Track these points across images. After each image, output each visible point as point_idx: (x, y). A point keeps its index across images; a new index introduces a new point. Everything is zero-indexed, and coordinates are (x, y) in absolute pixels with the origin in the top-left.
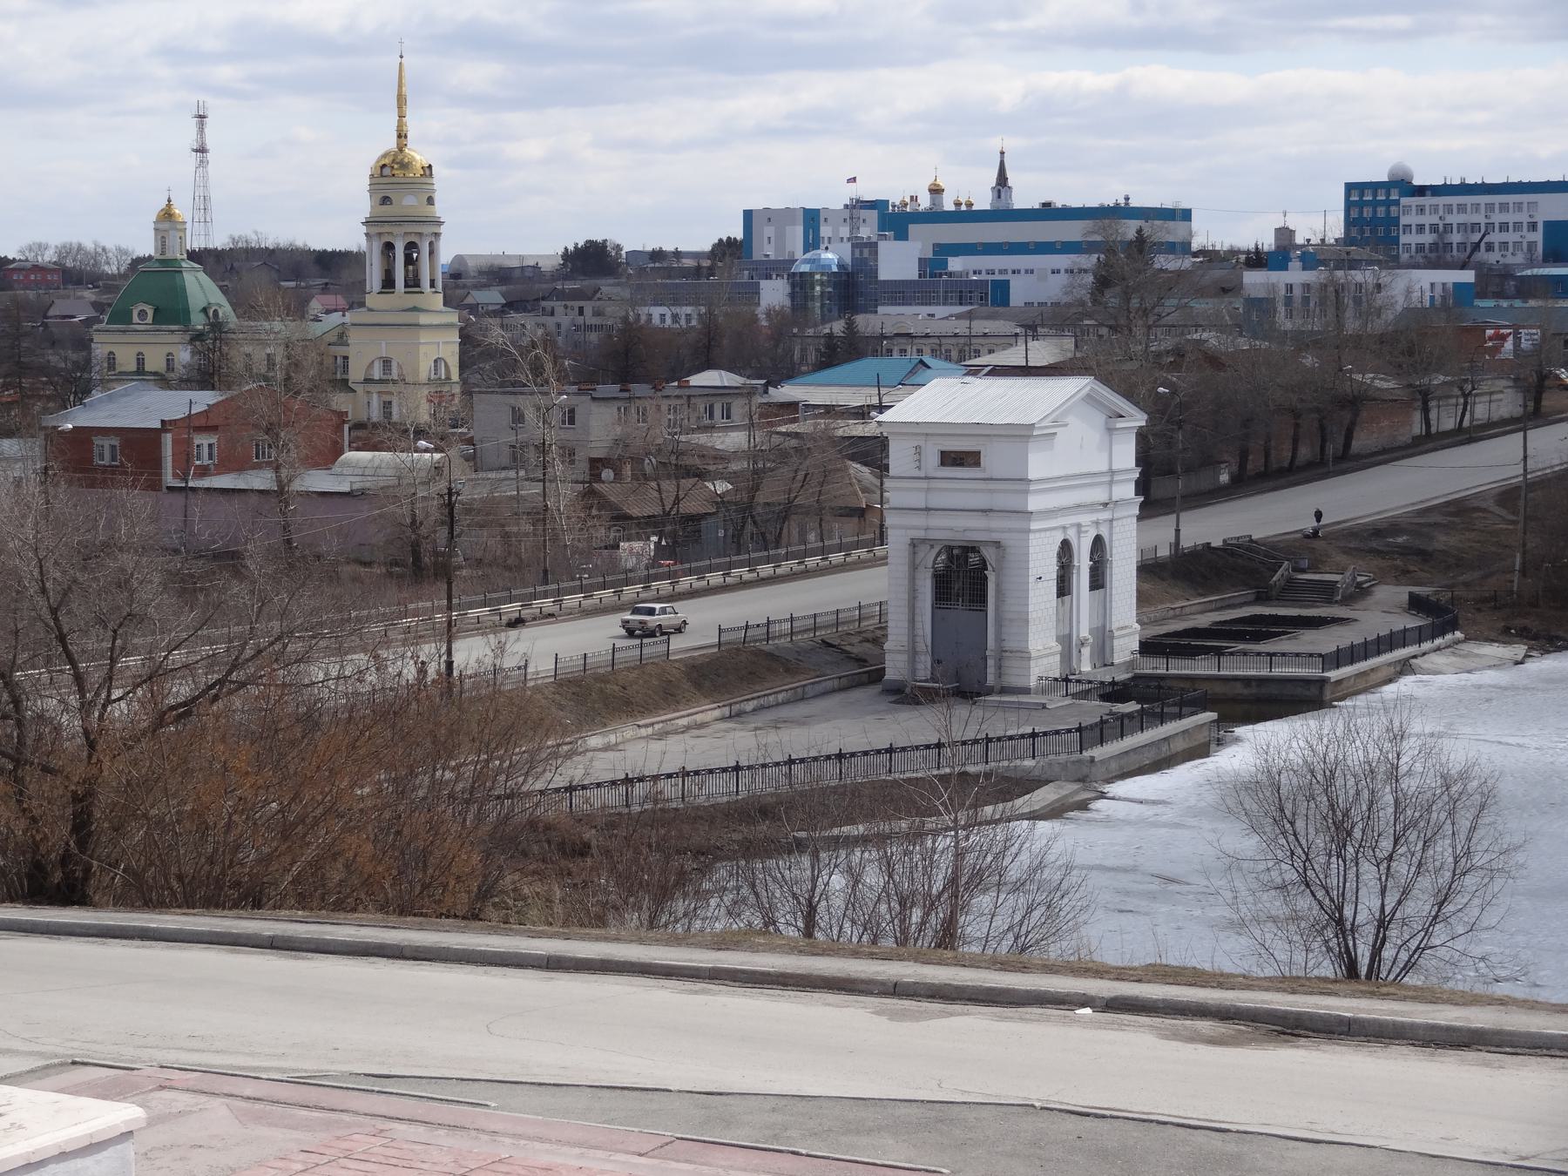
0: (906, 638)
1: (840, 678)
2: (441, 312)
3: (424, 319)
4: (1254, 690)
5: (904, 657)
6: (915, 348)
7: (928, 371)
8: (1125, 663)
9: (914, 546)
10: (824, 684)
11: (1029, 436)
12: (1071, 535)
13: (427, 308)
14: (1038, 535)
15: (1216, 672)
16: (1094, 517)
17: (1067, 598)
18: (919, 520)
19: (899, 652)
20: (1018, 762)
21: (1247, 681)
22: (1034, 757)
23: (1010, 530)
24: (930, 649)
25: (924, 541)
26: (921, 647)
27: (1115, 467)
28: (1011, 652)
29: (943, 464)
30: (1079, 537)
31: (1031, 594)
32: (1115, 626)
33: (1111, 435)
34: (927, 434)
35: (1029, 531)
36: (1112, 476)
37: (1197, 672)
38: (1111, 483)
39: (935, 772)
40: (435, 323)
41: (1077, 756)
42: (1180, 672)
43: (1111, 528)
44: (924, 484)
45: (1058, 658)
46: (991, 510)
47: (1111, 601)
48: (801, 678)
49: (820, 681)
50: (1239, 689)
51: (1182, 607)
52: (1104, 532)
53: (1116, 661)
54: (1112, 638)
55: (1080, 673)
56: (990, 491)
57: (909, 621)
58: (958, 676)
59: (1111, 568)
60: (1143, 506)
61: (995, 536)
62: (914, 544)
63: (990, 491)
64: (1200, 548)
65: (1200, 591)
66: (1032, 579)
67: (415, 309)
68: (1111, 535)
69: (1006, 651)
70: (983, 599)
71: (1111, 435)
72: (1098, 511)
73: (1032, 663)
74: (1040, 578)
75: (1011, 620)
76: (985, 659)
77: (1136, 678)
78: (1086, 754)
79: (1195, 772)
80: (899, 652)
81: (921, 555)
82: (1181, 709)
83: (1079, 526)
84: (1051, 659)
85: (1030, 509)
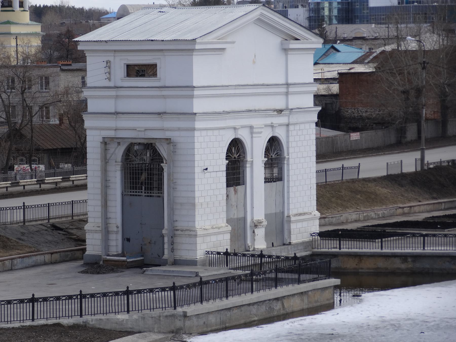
0: (99, 220)
1: (52, 254)
2: (28, 24)
3: (14, 29)
4: (409, 265)
5: (98, 236)
6: (367, 47)
7: (338, 54)
8: (303, 243)
9: (105, 143)
10: (34, 258)
11: (193, 50)
12: (244, 135)
13: (20, 22)
14: (204, 133)
15: (379, 250)
16: (268, 121)
17: (239, 188)
18: (110, 123)
19: (96, 231)
20: (112, 316)
21: (404, 257)
22: (128, 311)
23: (179, 129)
24: (120, 229)
25: (112, 139)
26: (113, 228)
27: (290, 82)
28: (182, 231)
29: (129, 75)
30: (252, 137)
31: (197, 182)
32: (292, 212)
33: (286, 55)
34: (115, 51)
35: (194, 129)
37: (364, 250)
38: (287, 94)
39: (28, 323)
40: (22, 32)
41: (170, 311)
42: (350, 250)
43: (288, 131)
44: (113, 93)
45: (228, 236)
46: (165, 113)
47: (288, 192)
48: (13, 253)
49: (31, 256)
50: (398, 264)
51: (411, 207)
52: (281, 134)
53: (294, 240)
54: (289, 222)
55: (254, 250)
56: (164, 97)
57: (102, 207)
58: (142, 253)
59: (288, 164)
60: (320, 115)
61: (168, 134)
62: (105, 142)
63: (164, 97)
64: (446, 164)
65: (435, 195)
66: (198, 170)
67: (8, 23)
68: (288, 137)
69: (177, 230)
70: (160, 188)
71: (286, 55)
72: (272, 116)
73: (199, 240)
74: (206, 169)
76: (163, 236)
77: (314, 256)
78: (180, 310)
79: (287, 326)
80: (96, 231)
81: (111, 150)
82: (299, 276)
83: (251, 127)
84: (220, 237)
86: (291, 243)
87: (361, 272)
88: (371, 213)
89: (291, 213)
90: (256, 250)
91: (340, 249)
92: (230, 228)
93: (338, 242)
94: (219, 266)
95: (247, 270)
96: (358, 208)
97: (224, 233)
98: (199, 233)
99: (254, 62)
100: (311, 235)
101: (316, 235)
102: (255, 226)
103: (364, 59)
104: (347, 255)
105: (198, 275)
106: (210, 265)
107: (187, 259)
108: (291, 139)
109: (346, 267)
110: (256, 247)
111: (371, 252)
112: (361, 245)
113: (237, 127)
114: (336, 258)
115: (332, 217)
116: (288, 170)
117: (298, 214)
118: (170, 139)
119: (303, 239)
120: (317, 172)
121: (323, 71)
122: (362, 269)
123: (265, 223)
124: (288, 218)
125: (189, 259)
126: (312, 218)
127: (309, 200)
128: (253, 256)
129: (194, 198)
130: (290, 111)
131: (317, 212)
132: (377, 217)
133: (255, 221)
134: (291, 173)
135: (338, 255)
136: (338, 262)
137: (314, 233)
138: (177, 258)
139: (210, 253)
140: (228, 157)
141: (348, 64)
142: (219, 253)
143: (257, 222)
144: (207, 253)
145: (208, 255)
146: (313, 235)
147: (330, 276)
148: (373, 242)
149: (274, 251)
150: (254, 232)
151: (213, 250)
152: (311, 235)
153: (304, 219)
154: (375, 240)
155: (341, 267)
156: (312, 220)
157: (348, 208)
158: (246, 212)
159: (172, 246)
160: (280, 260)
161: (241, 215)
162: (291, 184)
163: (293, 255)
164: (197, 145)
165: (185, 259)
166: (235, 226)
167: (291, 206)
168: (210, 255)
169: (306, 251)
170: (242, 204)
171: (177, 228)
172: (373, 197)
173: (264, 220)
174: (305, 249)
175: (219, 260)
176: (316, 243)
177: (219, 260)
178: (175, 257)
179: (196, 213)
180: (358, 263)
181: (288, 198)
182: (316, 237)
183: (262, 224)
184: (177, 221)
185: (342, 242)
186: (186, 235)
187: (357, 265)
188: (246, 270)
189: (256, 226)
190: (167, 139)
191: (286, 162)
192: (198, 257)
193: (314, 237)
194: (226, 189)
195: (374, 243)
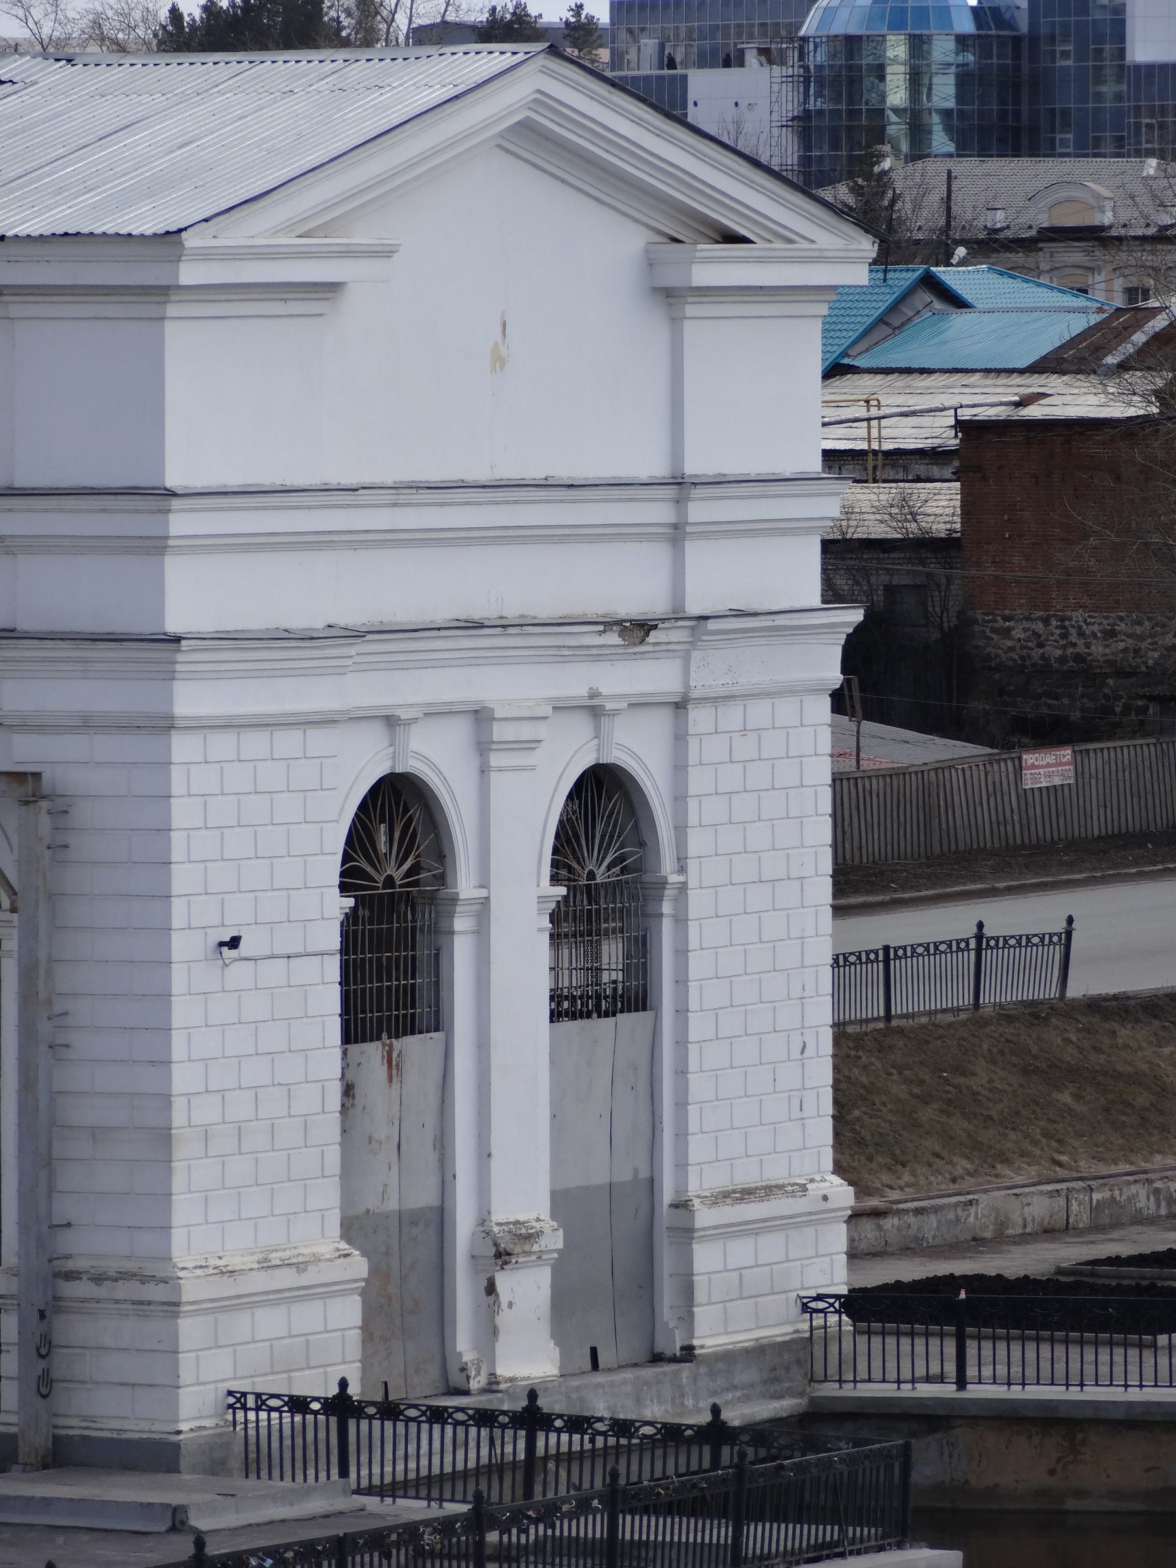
6: (1119, 284)
7: (960, 320)
8: (759, 1352)
11: (163, 292)
14: (222, 745)
17: (413, 1047)
23: (86, 724)
27: (692, 468)
28: (98, 1279)
30: (484, 770)
31: (182, 1012)
33: (676, 322)
35: (165, 725)
36: (680, 502)
37: (1093, 1393)
42: (1016, 1392)
43: (680, 737)
47: (682, 1072)
54: (686, 1234)
59: (681, 921)
68: (680, 768)
69: (72, 1276)
71: (676, 322)
72: (595, 655)
73: (190, 1330)
74: (234, 943)
75: (97, 1133)
83: (481, 716)
84: (308, 1316)
85: (173, 626)
86: (697, 1352)
87: (1076, 1512)
88: (1134, 1189)
89: (693, 1188)
90: (502, 1386)
91: (961, 1383)
92: (359, 1266)
93: (951, 1348)
94: (299, 1477)
95: (452, 1500)
96: (1064, 1158)
97: (326, 1292)
98: (191, 1290)
99: (499, 361)
100: (805, 1305)
101: (832, 1305)
102: (498, 1255)
103: (1100, 350)
104: (998, 1418)
105: (183, 1523)
106: (253, 1467)
107: (125, 1436)
108: (697, 781)
109: (996, 1485)
110: (503, 1371)
111: (1130, 1405)
112: (1075, 1366)
113: (404, 715)
114: (938, 1436)
115: (919, 1212)
116: (682, 952)
117: (734, 1192)
118: (37, 776)
119: (758, 1328)
120: (840, 962)
121: (874, 412)
122: (1081, 1494)
123: (553, 1240)
124: (681, 1211)
125: (137, 1436)
126: (810, 1213)
127: (796, 1113)
128: (485, 1418)
129: (165, 1099)
130: (693, 628)
131: (837, 1180)
132: (1163, 1211)
133: (496, 1229)
134: (698, 965)
135: (954, 1417)
136: (951, 1456)
137: (819, 1298)
138: (71, 1432)
139: (251, 1402)
140: (350, 881)
141: (1011, 371)
142: (298, 1404)
143: (508, 1237)
144: (231, 1400)
145: (240, 1415)
146: (813, 1305)
147: (904, 1534)
148: (1141, 1346)
149: (600, 1391)
150: (491, 1289)
151: (265, 1385)
152: (805, 1308)
153: (765, 1220)
154: (1154, 1335)
155: (967, 1482)
156: (808, 1223)
157: (1007, 1161)
158: (448, 1177)
159: (42, 1364)
160: (635, 1441)
161: (424, 1197)
162: (698, 1027)
163: (705, 1418)
164: (182, 813)
165: (115, 1435)
166: (387, 1254)
167: (698, 1149)
168: (252, 1415)
169: (779, 1396)
170: (429, 1134)
171: (70, 1265)
172: (1143, 1099)
173: (548, 1224)
174: (772, 1385)
175: (299, 1441)
176: (833, 1349)
177: (299, 1441)
178: (61, 1422)
179: (178, 1183)
180: (1059, 1460)
181: (682, 1104)
182: (833, 1319)
183: (536, 1248)
184: (69, 1225)
185: (971, 1348)
186: (117, 1302)
187: (1052, 1472)
188: (448, 1495)
189: (502, 1256)
190: (19, 777)
191: (667, 908)
192: (184, 1427)
193: (818, 1320)
194: (338, 1052)
195: (1148, 1355)
